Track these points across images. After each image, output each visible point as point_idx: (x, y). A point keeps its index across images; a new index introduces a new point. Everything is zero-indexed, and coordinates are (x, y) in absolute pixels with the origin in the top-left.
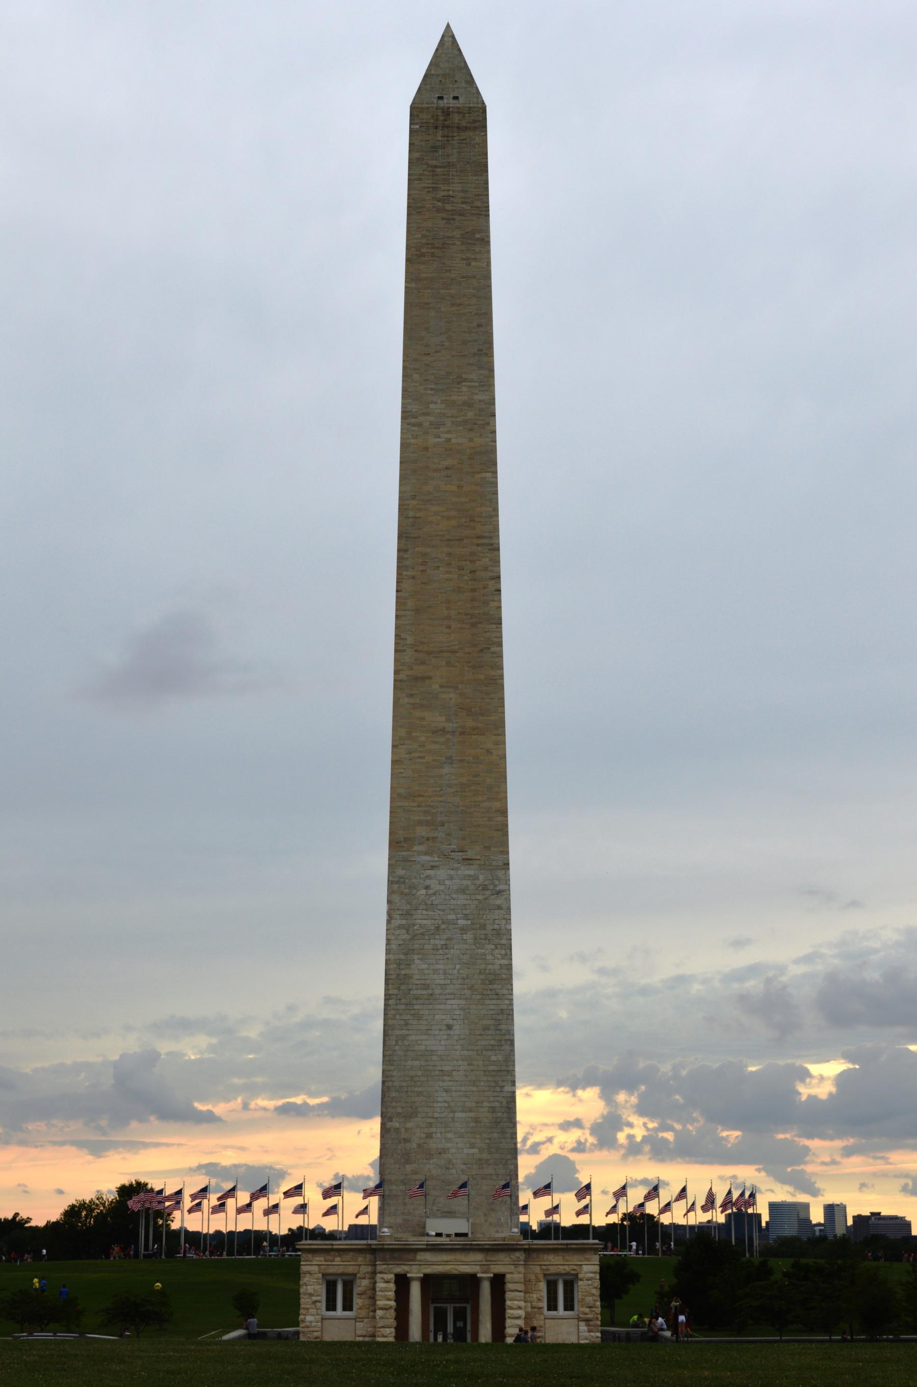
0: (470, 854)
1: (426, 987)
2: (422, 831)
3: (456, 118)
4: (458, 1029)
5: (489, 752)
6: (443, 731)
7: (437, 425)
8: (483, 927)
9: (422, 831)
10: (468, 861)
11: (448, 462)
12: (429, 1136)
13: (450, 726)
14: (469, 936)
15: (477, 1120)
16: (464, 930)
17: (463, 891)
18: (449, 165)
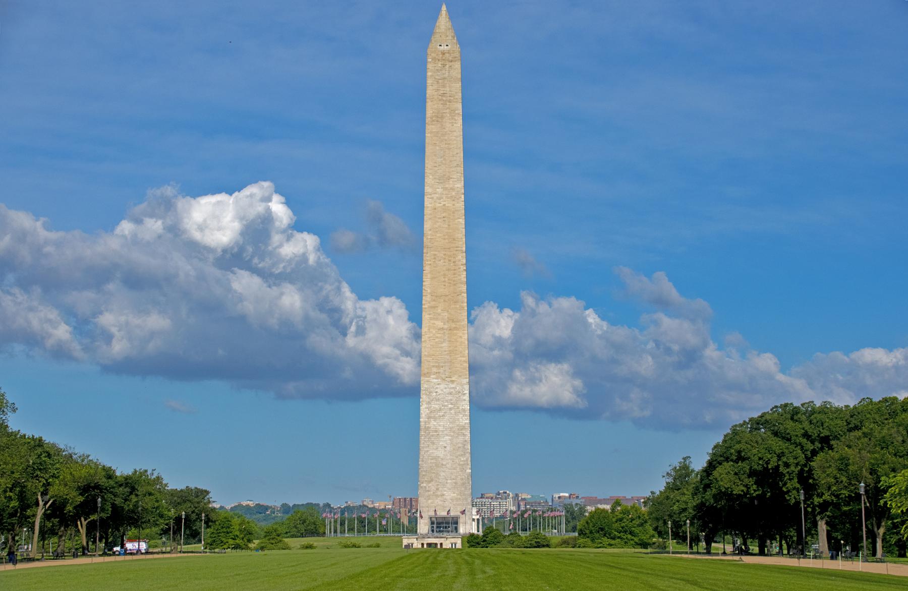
0: (453, 379)
1: (436, 431)
2: (435, 370)
3: (447, 55)
4: (448, 448)
5: (461, 337)
6: (443, 329)
7: (440, 198)
8: (458, 408)
9: (435, 370)
10: (453, 382)
11: (444, 215)
12: (437, 489)
13: (446, 327)
14: (453, 412)
15: (456, 483)
16: (450, 409)
17: (451, 393)
18: (444, 78)
